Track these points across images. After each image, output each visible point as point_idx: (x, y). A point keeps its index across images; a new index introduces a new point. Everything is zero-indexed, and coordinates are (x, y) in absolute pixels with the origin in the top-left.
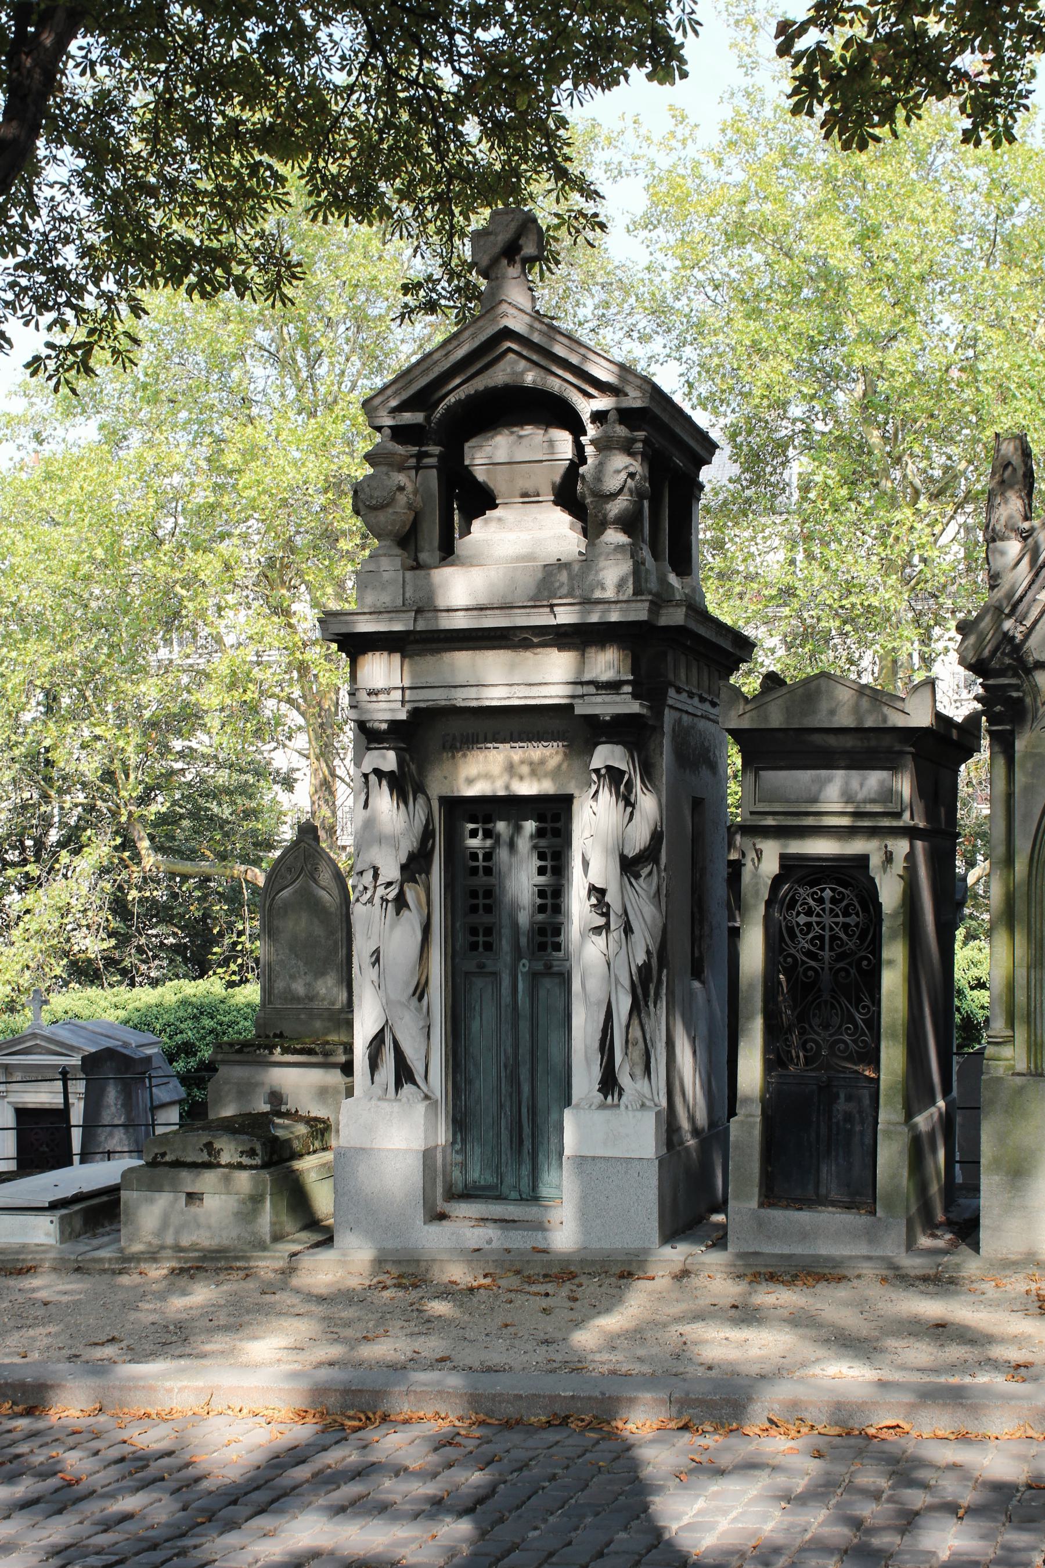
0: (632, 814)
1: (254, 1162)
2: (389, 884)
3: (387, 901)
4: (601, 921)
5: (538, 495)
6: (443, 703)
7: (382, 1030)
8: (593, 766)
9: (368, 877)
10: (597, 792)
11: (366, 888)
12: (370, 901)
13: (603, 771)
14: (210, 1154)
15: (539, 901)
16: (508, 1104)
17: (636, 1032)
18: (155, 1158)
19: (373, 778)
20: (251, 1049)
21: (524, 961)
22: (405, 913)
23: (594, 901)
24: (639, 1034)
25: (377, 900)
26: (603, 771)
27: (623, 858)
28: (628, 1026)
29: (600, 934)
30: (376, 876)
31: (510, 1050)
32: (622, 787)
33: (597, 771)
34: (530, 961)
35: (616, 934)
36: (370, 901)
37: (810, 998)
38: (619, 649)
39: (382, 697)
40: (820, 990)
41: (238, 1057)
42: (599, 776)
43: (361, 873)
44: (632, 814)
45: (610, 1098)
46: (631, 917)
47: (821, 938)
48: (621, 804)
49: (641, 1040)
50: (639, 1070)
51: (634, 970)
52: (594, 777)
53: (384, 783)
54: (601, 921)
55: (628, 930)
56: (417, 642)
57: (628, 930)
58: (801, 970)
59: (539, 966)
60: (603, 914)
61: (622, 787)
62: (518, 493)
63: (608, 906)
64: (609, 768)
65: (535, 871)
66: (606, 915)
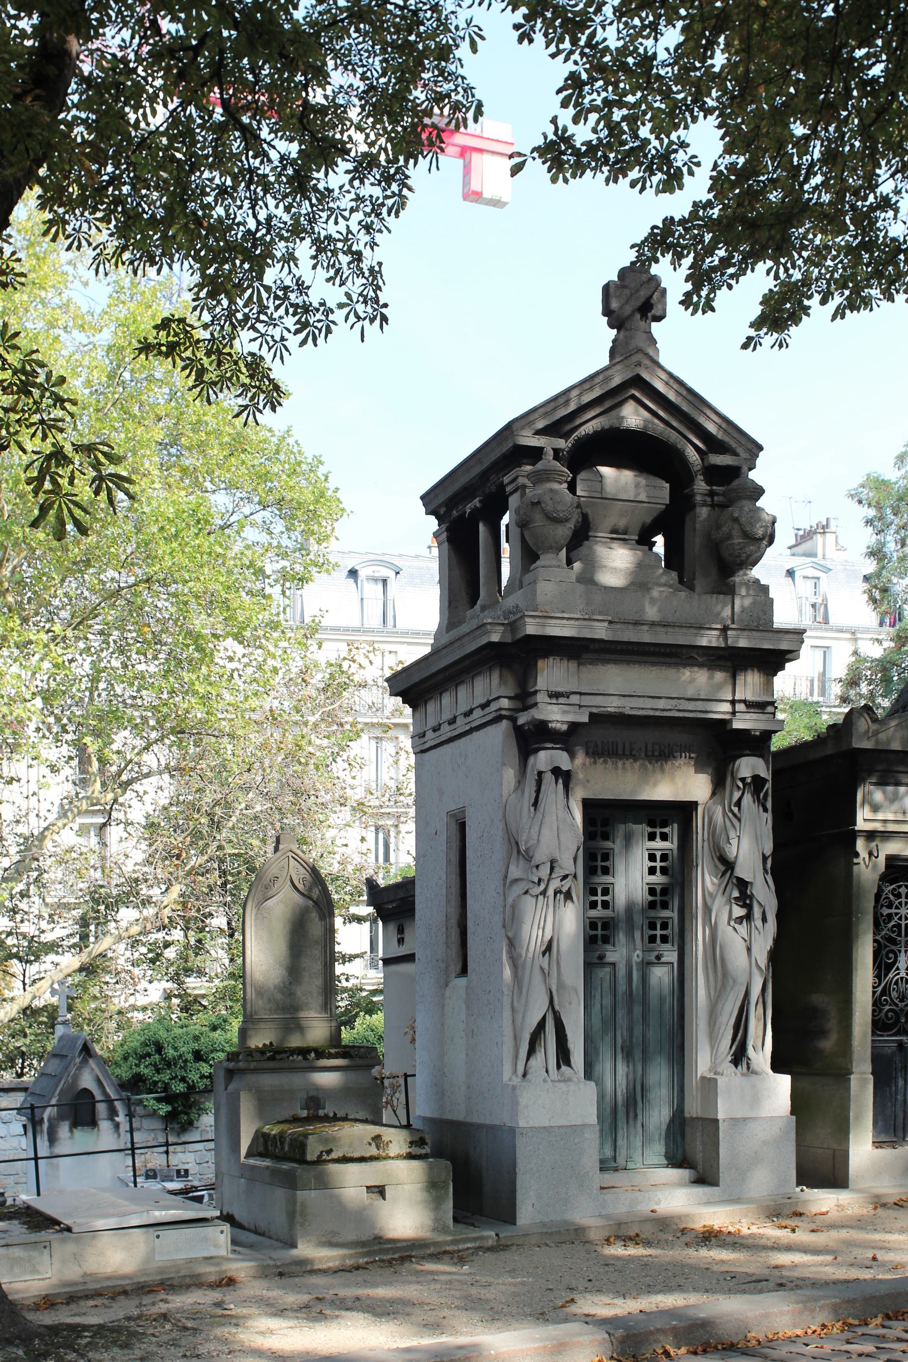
1: (423, 1152)
2: (565, 877)
3: (561, 892)
5: (625, 534)
7: (544, 1018)
9: (544, 872)
11: (540, 880)
12: (544, 893)
14: (378, 1148)
15: (650, 898)
18: (321, 1155)
19: (549, 778)
20: (284, 1055)
22: (569, 904)
23: (736, 894)
25: (551, 892)
29: (741, 923)
30: (552, 869)
32: (762, 795)
33: (743, 780)
36: (544, 893)
37: (890, 975)
38: (759, 671)
40: (898, 969)
41: (272, 1064)
43: (537, 867)
47: (898, 926)
48: (761, 809)
52: (741, 785)
53: (560, 781)
55: (764, 920)
56: (597, 651)
57: (764, 920)
58: (884, 952)
60: (744, 906)
61: (762, 795)
62: (609, 529)
65: (646, 871)
66: (749, 908)
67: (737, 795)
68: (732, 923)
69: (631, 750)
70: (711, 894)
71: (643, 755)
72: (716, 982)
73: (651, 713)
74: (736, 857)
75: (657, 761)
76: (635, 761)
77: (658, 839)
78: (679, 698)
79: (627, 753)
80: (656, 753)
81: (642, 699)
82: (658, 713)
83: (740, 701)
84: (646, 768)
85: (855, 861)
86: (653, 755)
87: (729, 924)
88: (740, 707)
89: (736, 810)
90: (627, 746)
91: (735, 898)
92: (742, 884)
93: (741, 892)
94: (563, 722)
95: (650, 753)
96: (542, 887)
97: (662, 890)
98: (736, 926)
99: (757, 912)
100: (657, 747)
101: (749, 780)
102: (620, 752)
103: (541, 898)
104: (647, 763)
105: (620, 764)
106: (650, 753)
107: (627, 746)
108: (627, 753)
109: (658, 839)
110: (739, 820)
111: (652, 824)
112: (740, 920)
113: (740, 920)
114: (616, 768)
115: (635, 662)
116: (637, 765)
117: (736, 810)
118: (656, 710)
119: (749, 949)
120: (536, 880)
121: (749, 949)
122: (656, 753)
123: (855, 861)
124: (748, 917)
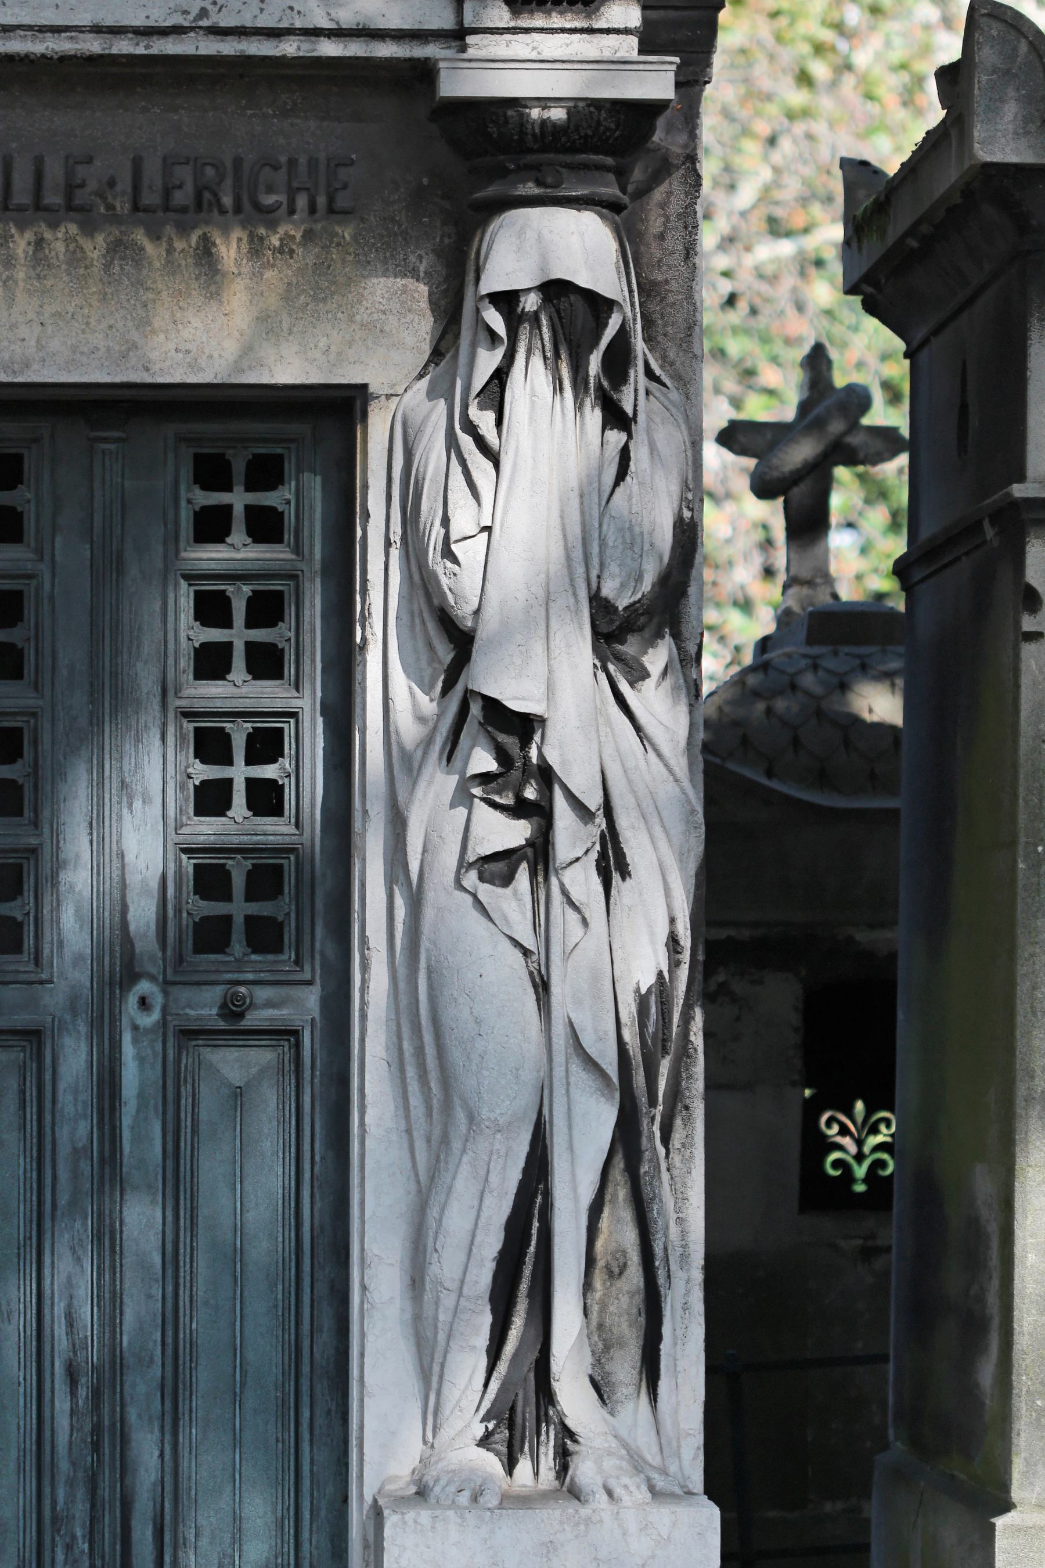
0: (625, 455)
4: (515, 833)
8: (494, 280)
10: (500, 376)
13: (531, 303)
16: (81, 1509)
17: (619, 1231)
21: (144, 987)
23: (483, 761)
24: (630, 1237)
26: (531, 303)
27: (600, 606)
28: (596, 1210)
29: (507, 880)
32: (594, 363)
33: (506, 301)
34: (166, 985)
35: (582, 881)
42: (514, 318)
44: (625, 455)
45: (524, 1466)
46: (623, 822)
48: (594, 417)
49: (634, 1258)
50: (625, 1368)
51: (629, 1010)
52: (495, 320)
54: (515, 833)
55: (612, 863)
57: (612, 863)
59: (204, 1006)
60: (520, 809)
63: (546, 775)
64: (555, 290)
65: (186, 664)
66: (540, 813)
67: (488, 361)
69: (71, 188)
70: (406, 757)
71: (122, 206)
72: (429, 1114)
73: (94, 45)
75: (184, 230)
76: (89, 228)
77: (238, 535)
79: (53, 198)
82: (124, 46)
84: (138, 257)
85: (1028, 623)
87: (459, 885)
89: (485, 421)
90: (55, 172)
91: (485, 778)
93: (502, 756)
95: (151, 198)
97: (252, 739)
98: (485, 891)
99: (571, 837)
100: (185, 174)
102: (21, 195)
104: (140, 236)
106: (151, 198)
107: (55, 172)
108: (53, 198)
109: (238, 535)
111: (212, 473)
113: (498, 867)
116: (95, 248)
119: (542, 986)
121: (542, 986)
122: (180, 198)
123: (1028, 623)
124: (539, 854)
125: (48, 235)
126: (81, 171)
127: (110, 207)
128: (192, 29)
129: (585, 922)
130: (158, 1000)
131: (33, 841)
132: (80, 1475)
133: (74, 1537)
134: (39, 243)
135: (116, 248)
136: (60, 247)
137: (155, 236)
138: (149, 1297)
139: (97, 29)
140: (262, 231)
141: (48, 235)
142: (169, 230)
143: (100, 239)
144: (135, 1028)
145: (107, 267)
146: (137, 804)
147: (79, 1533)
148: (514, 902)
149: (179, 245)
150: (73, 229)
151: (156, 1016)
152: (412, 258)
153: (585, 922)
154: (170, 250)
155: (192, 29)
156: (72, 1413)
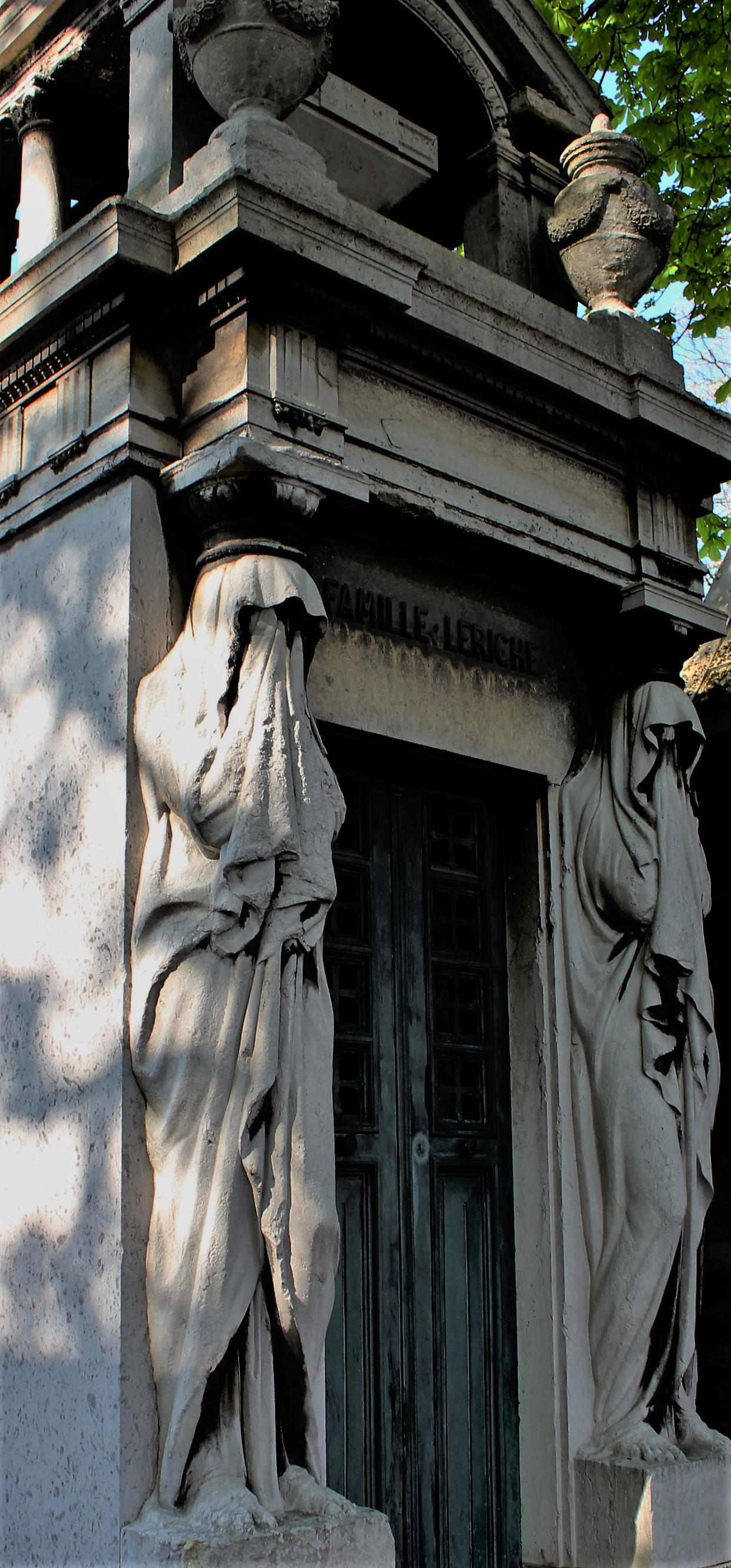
6: (411, 499)
12: (253, 949)
23: (654, 998)
25: (271, 949)
29: (665, 1071)
31: (401, 1355)
36: (253, 949)
39: (305, 435)
53: (298, 642)
66: (680, 1032)
68: (651, 1071)
71: (440, 646)
73: (487, 530)
74: (655, 909)
75: (468, 666)
76: (426, 654)
78: (538, 514)
80: (467, 646)
81: (467, 493)
82: (499, 535)
83: (650, 554)
84: (449, 679)
86: (460, 650)
88: (649, 566)
89: (642, 799)
91: (652, 1010)
92: (669, 973)
94: (311, 486)
96: (252, 928)
100: (467, 633)
101: (670, 735)
102: (395, 626)
103: (243, 960)
104: (448, 664)
105: (395, 653)
110: (653, 823)
112: (663, 1064)
113: (663, 1064)
114: (388, 663)
115: (452, 404)
116: (429, 665)
117: (642, 799)
118: (495, 524)
120: (236, 907)
122: (467, 646)
125: (407, 652)
126: (423, 618)
127: (435, 644)
128: (528, 535)
129: (705, 1096)
130: (427, 1147)
131: (368, 1039)
132: (397, 1462)
133: (395, 1505)
134: (404, 655)
135: (439, 667)
136: (412, 659)
137: (455, 666)
138: (427, 1340)
139: (488, 521)
140: (500, 676)
141: (407, 652)
142: (461, 665)
143: (431, 661)
144: (417, 1164)
145: (435, 678)
146: (414, 1020)
147: (397, 1502)
148: (672, 1081)
149: (466, 674)
150: (419, 652)
151: (426, 1157)
152: (561, 709)
153: (705, 1096)
154: (462, 676)
155: (528, 535)
156: (394, 1420)
